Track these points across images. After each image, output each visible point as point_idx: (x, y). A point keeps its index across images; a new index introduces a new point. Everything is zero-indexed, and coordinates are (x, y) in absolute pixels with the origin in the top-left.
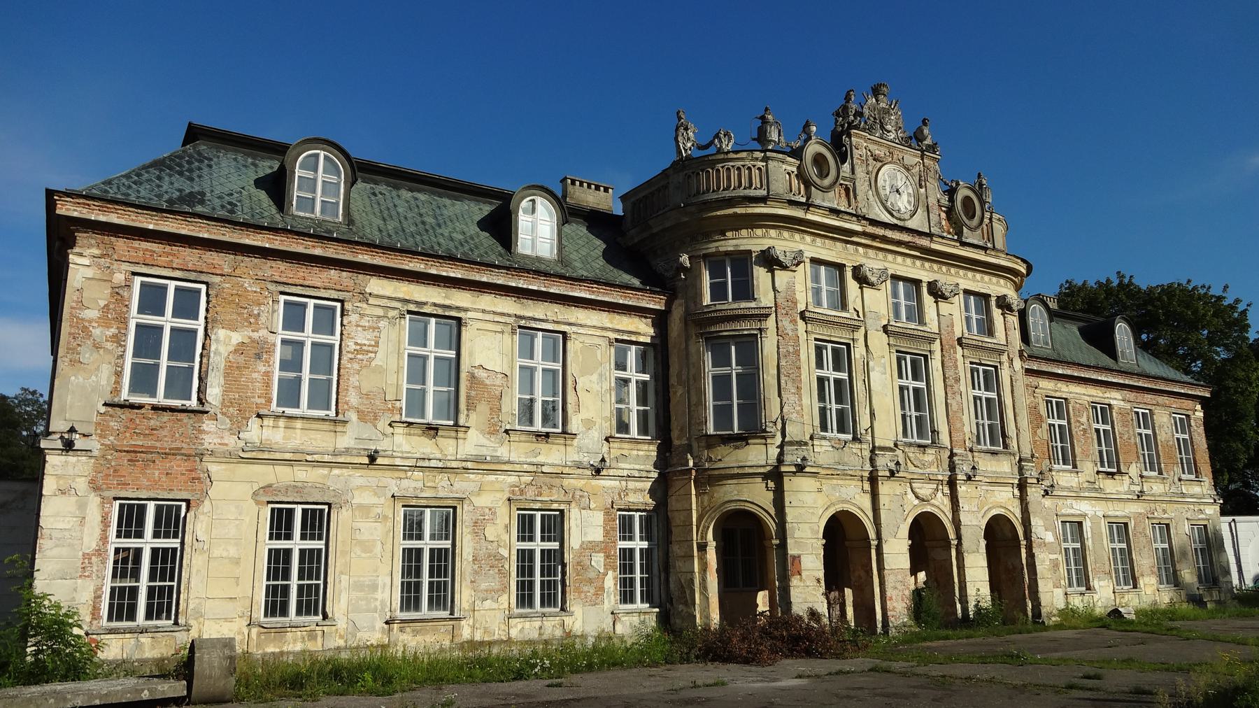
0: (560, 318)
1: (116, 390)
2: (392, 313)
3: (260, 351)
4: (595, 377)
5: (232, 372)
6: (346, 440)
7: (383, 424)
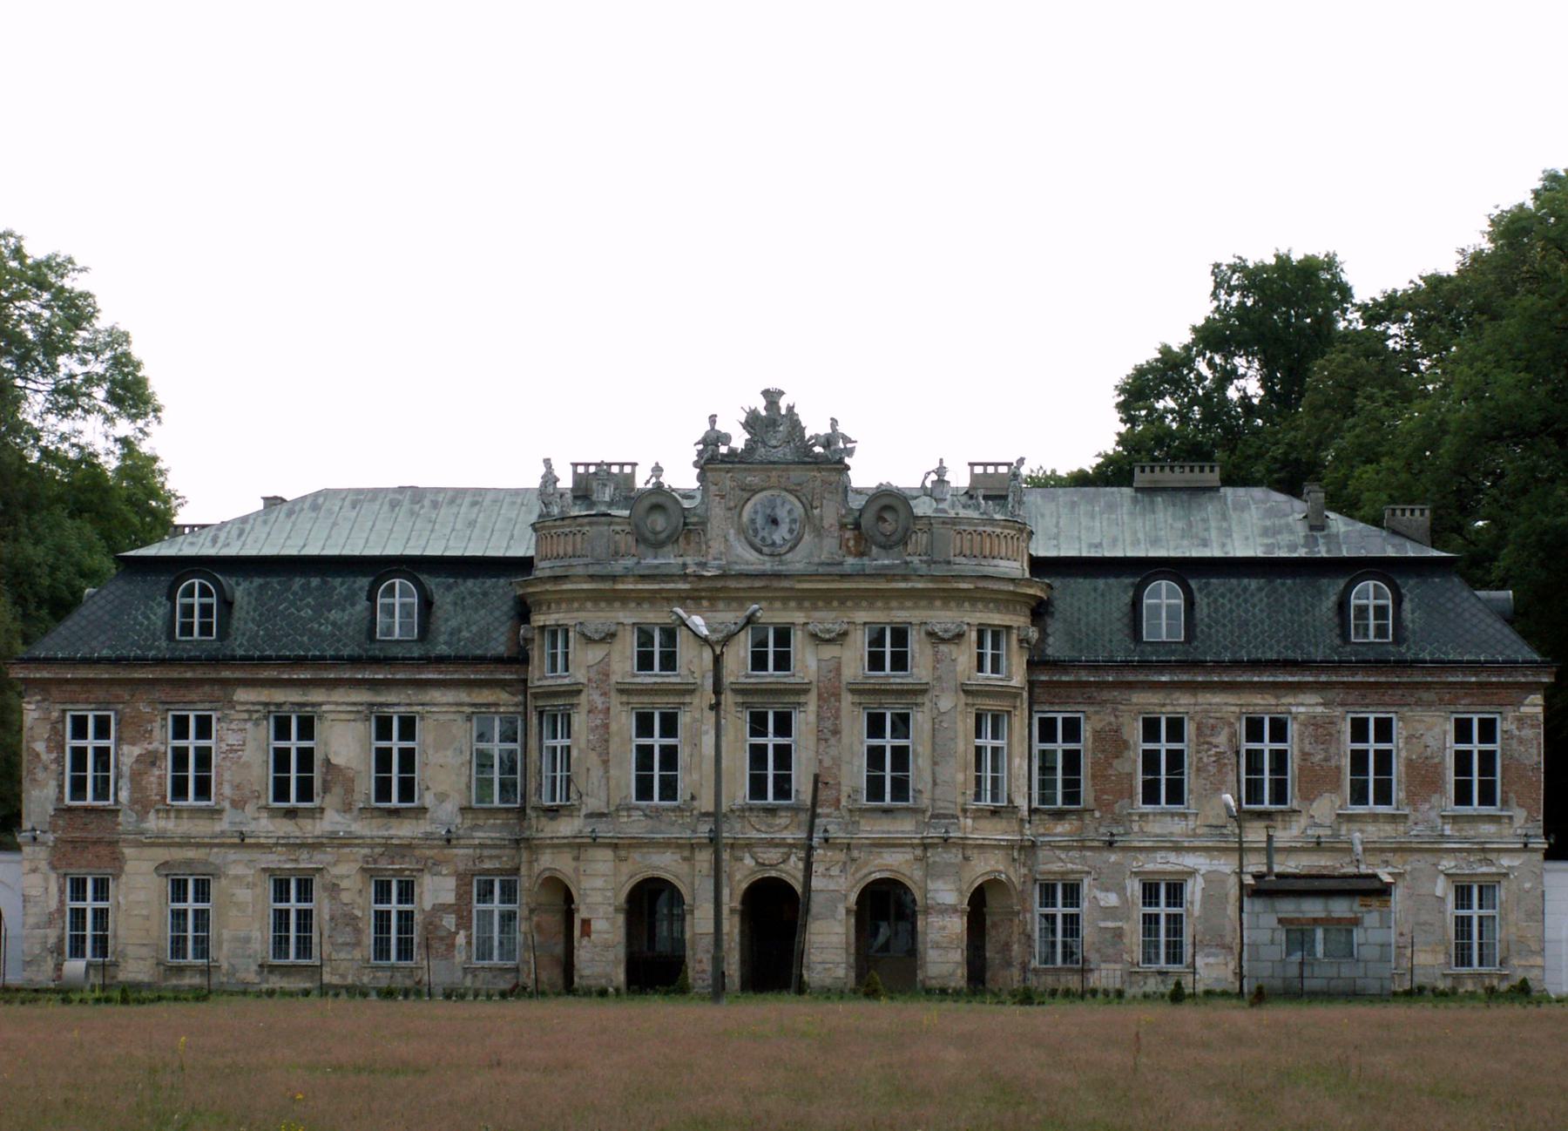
0: (414, 699)
1: (60, 799)
2: (255, 716)
3: (152, 759)
4: (449, 753)
5: (136, 778)
6: (223, 825)
7: (250, 809)
